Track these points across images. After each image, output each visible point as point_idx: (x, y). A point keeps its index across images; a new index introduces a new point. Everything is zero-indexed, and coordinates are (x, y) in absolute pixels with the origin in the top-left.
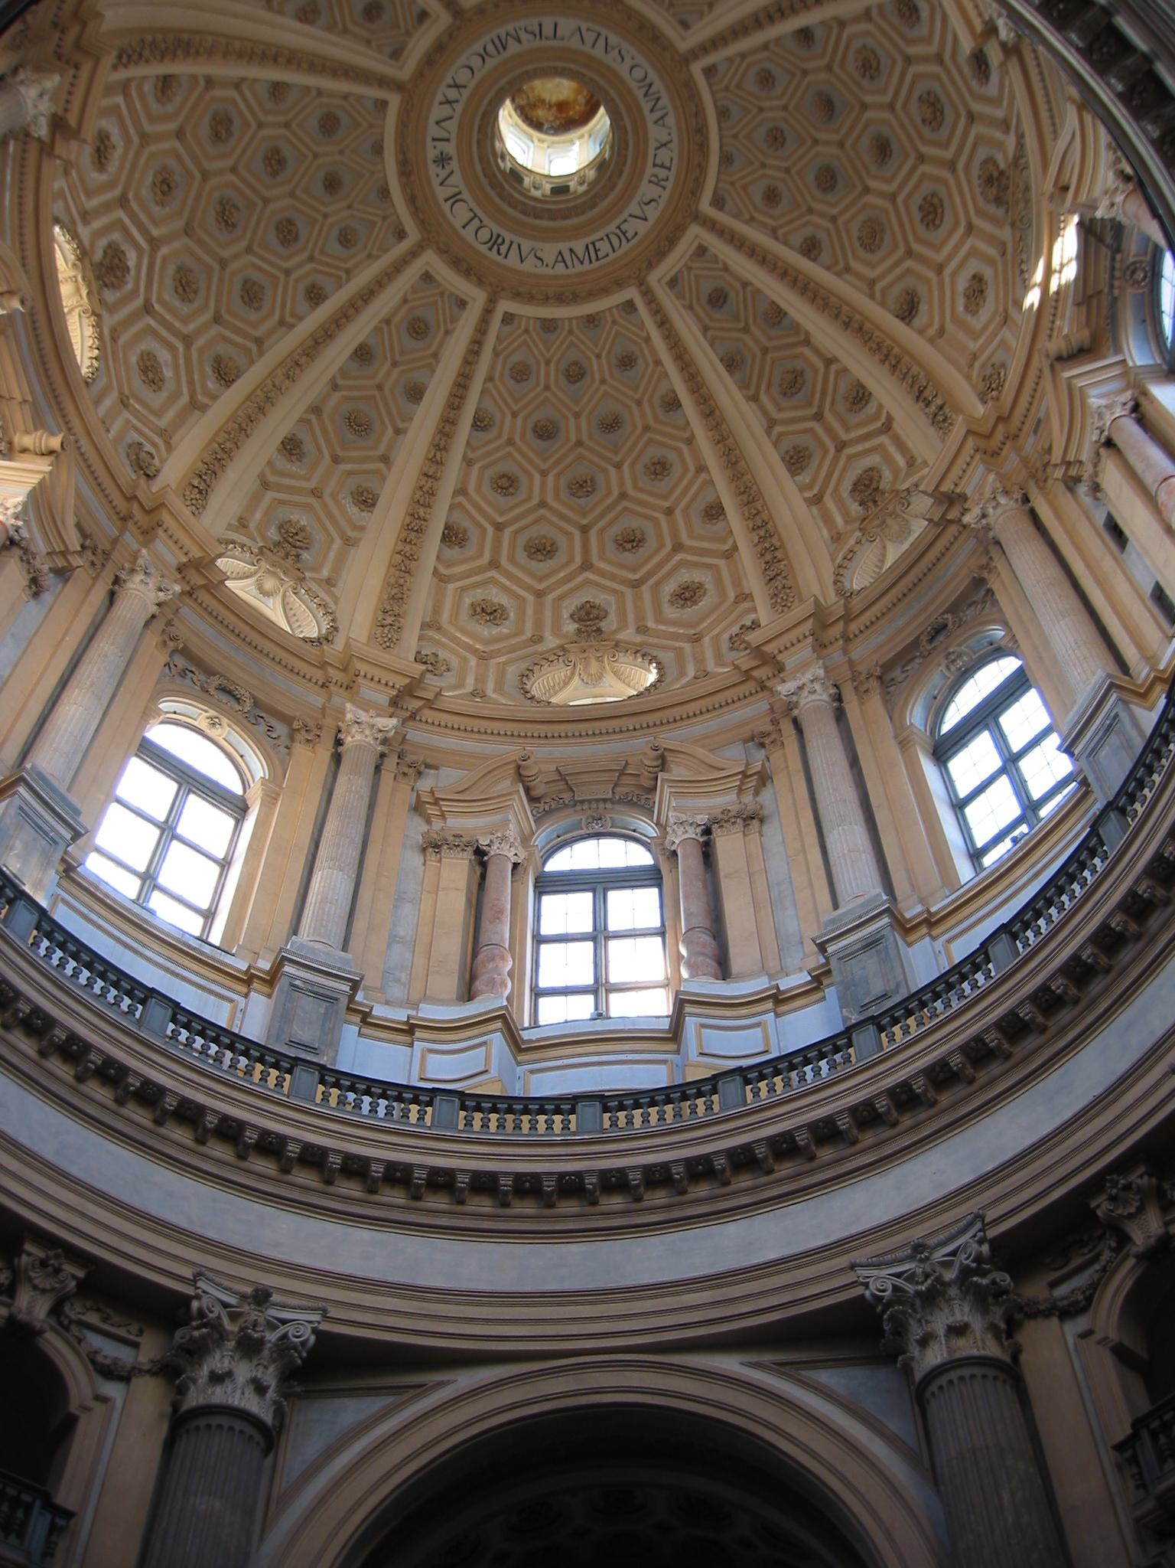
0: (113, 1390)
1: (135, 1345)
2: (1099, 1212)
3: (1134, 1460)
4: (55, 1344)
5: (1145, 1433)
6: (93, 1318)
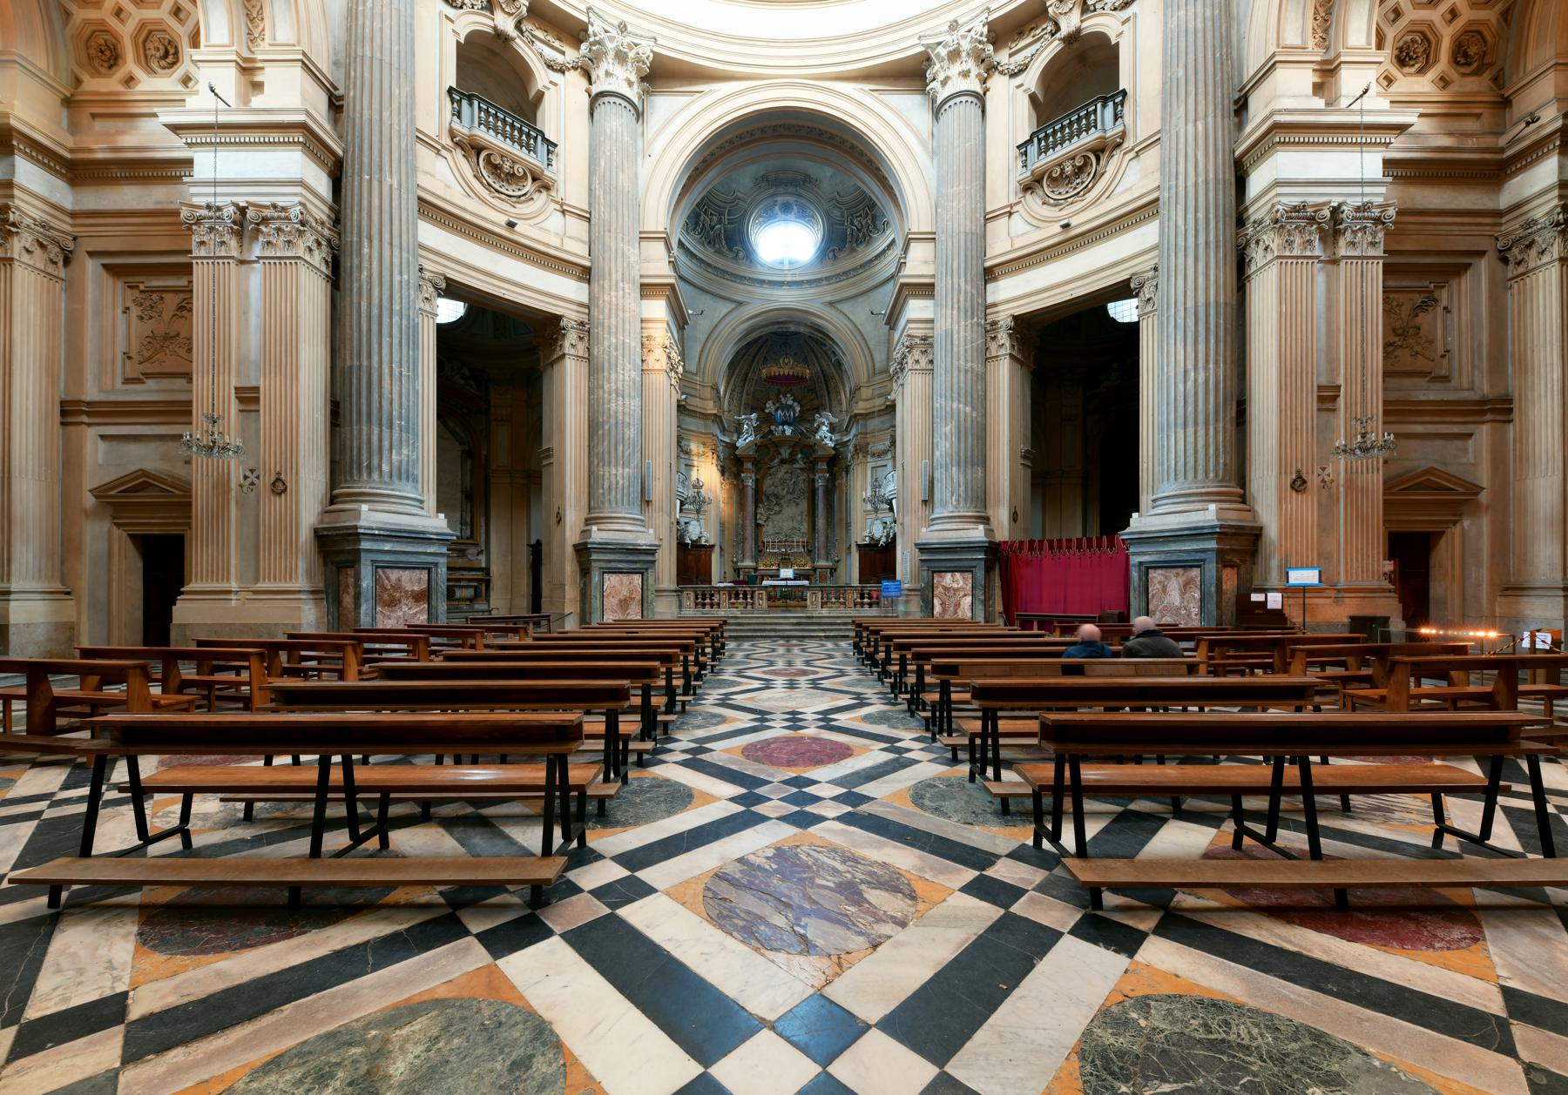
0: (556, 77)
1: (563, 53)
2: (1050, 10)
3: (1025, 153)
4: (521, 46)
5: (1035, 140)
6: (539, 34)
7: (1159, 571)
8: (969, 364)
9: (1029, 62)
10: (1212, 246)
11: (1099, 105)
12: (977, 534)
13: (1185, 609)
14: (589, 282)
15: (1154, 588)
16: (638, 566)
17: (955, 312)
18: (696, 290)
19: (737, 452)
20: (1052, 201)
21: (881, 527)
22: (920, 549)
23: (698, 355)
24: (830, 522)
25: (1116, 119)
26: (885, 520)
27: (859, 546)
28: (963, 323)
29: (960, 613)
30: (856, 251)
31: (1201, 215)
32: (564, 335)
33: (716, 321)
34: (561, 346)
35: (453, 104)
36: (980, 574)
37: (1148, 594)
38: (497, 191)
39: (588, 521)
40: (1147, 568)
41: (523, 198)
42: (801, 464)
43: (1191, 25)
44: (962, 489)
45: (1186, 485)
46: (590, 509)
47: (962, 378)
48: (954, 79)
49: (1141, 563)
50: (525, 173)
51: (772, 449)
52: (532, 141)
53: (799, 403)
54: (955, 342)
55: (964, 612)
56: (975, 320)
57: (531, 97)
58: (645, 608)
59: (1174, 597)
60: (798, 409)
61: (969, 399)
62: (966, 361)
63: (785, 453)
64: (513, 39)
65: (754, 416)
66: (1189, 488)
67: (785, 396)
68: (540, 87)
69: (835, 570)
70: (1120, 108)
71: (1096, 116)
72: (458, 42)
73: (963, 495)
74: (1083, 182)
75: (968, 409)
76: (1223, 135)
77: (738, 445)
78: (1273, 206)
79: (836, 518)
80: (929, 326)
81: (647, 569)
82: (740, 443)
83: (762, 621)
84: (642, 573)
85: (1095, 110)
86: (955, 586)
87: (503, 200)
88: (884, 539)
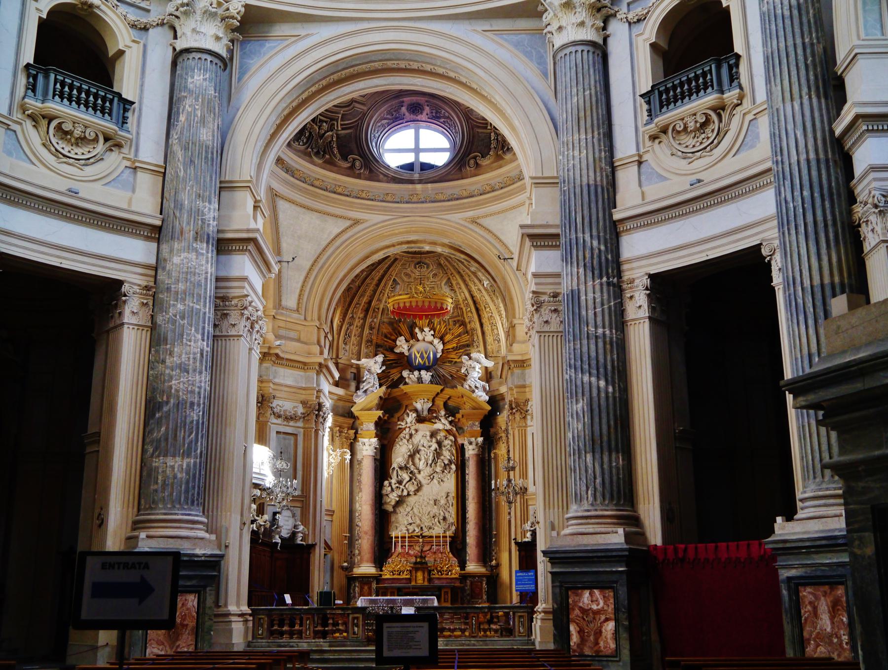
7: (809, 589)
8: (600, 331)
9: (648, 13)
10: (821, 225)
11: (713, 66)
12: (616, 538)
13: (837, 637)
14: (158, 241)
15: (805, 611)
16: (194, 582)
17: (581, 270)
18: (299, 209)
20: (680, 153)
22: (551, 559)
23: (299, 285)
25: (732, 80)
27: (516, 543)
28: (590, 283)
29: (602, 644)
30: (503, 158)
31: (806, 193)
32: (125, 302)
33: (324, 243)
34: (120, 313)
35: (28, 78)
36: (623, 591)
37: (801, 617)
38: (64, 156)
39: (137, 525)
40: (795, 584)
41: (92, 160)
43: (779, 12)
44: (598, 481)
45: (824, 486)
46: (139, 510)
47: (593, 347)
48: (569, 28)
49: (789, 579)
50: (97, 135)
52: (108, 104)
53: (442, 339)
54: (583, 303)
55: (606, 642)
56: (605, 279)
57: (110, 56)
58: (199, 639)
59: (825, 622)
61: (602, 370)
62: (596, 327)
64: (98, 7)
65: (380, 358)
66: (827, 489)
67: (422, 330)
68: (121, 47)
70: (734, 70)
71: (711, 75)
72: (40, 18)
73: (599, 488)
74: (708, 138)
75: (602, 383)
76: (821, 116)
78: (870, 193)
80: (557, 280)
81: (205, 587)
83: (355, 656)
84: (199, 593)
85: (710, 70)
86: (595, 607)
87: (70, 164)
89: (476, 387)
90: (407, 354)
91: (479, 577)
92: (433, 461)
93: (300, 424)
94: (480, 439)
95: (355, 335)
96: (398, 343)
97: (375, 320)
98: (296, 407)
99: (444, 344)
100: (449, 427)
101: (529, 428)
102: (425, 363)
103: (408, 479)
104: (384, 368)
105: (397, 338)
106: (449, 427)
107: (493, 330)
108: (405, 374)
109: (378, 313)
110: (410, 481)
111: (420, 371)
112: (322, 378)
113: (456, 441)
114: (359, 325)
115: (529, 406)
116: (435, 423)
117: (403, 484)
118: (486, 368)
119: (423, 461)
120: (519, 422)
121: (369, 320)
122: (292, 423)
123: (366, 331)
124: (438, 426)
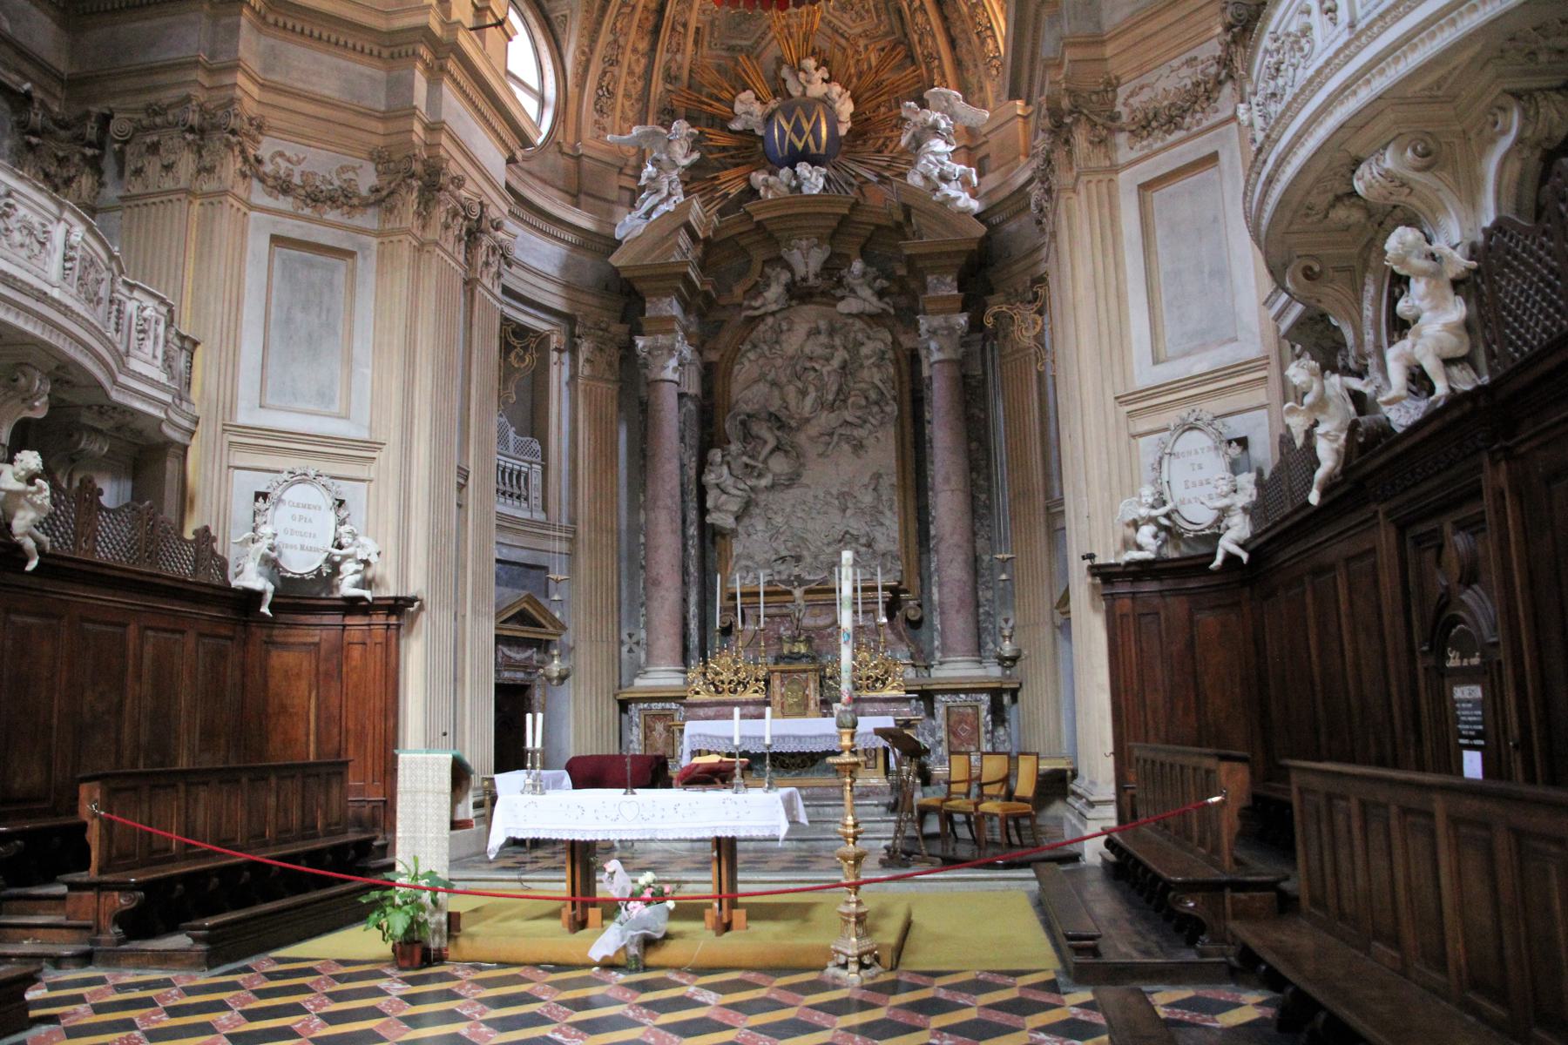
19: (617, 260)
21: (1215, 466)
24: (978, 508)
26: (1237, 426)
42: (863, 299)
51: (759, 255)
60: (846, 108)
63: (807, 260)
65: (681, 127)
67: (797, 69)
69: (1014, 694)
77: (619, 234)
79: (1003, 499)
82: (629, 225)
88: (1237, 531)
89: (944, 178)
90: (759, 132)
91: (967, 691)
92: (838, 394)
93: (369, 219)
94: (962, 320)
95: (627, 96)
96: (738, 108)
97: (679, 57)
98: (354, 169)
99: (855, 99)
100: (873, 304)
101: (1123, 177)
102: (806, 145)
103: (772, 443)
104: (696, 156)
105: (734, 97)
106: (873, 304)
107: (983, 42)
108: (758, 178)
109: (685, 35)
110: (777, 448)
111: (793, 167)
112: (447, 90)
113: (896, 343)
114: (639, 69)
115: (1120, 100)
116: (843, 298)
117: (761, 458)
118: (970, 132)
119: (813, 394)
120: (1088, 158)
121: (662, 57)
122: (332, 215)
123: (658, 86)
124: (848, 306)
